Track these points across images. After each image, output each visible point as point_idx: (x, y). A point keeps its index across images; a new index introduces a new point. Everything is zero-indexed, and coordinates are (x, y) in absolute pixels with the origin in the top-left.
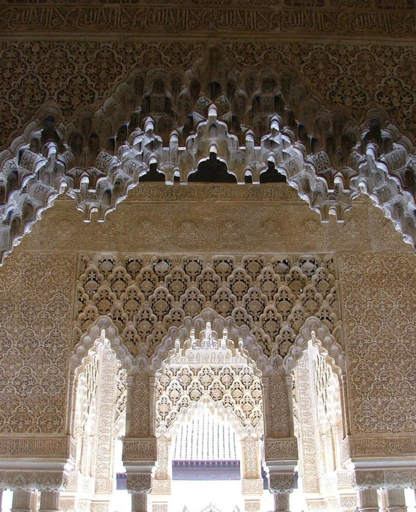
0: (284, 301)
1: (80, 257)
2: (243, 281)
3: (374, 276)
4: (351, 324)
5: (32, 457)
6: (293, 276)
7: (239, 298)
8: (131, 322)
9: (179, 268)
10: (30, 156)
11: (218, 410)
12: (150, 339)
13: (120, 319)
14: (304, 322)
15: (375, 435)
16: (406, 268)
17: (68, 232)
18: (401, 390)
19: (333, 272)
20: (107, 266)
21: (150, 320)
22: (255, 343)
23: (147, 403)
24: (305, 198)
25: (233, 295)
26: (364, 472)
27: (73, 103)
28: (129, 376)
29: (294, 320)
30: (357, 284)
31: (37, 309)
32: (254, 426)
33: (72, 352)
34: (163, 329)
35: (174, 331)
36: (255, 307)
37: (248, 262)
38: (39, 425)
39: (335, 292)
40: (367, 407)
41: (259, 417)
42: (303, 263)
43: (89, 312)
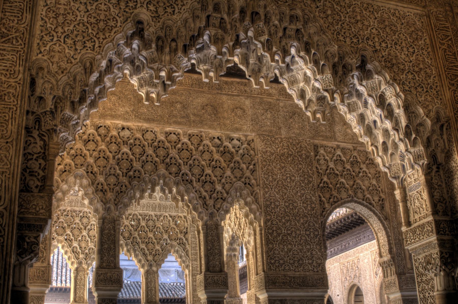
0: (218, 168)
2: (187, 150)
3: (283, 155)
4: (267, 190)
6: (224, 150)
7: (185, 163)
8: (101, 176)
10: (122, 49)
11: (127, 247)
13: (92, 172)
15: (283, 273)
16: (305, 151)
18: (300, 241)
22: (196, 199)
24: (301, 103)
25: (180, 161)
26: (274, 300)
27: (159, 13)
29: (225, 183)
30: (271, 160)
34: (127, 183)
36: (197, 171)
39: (254, 165)
40: (277, 252)
41: (159, 254)
43: (66, 165)
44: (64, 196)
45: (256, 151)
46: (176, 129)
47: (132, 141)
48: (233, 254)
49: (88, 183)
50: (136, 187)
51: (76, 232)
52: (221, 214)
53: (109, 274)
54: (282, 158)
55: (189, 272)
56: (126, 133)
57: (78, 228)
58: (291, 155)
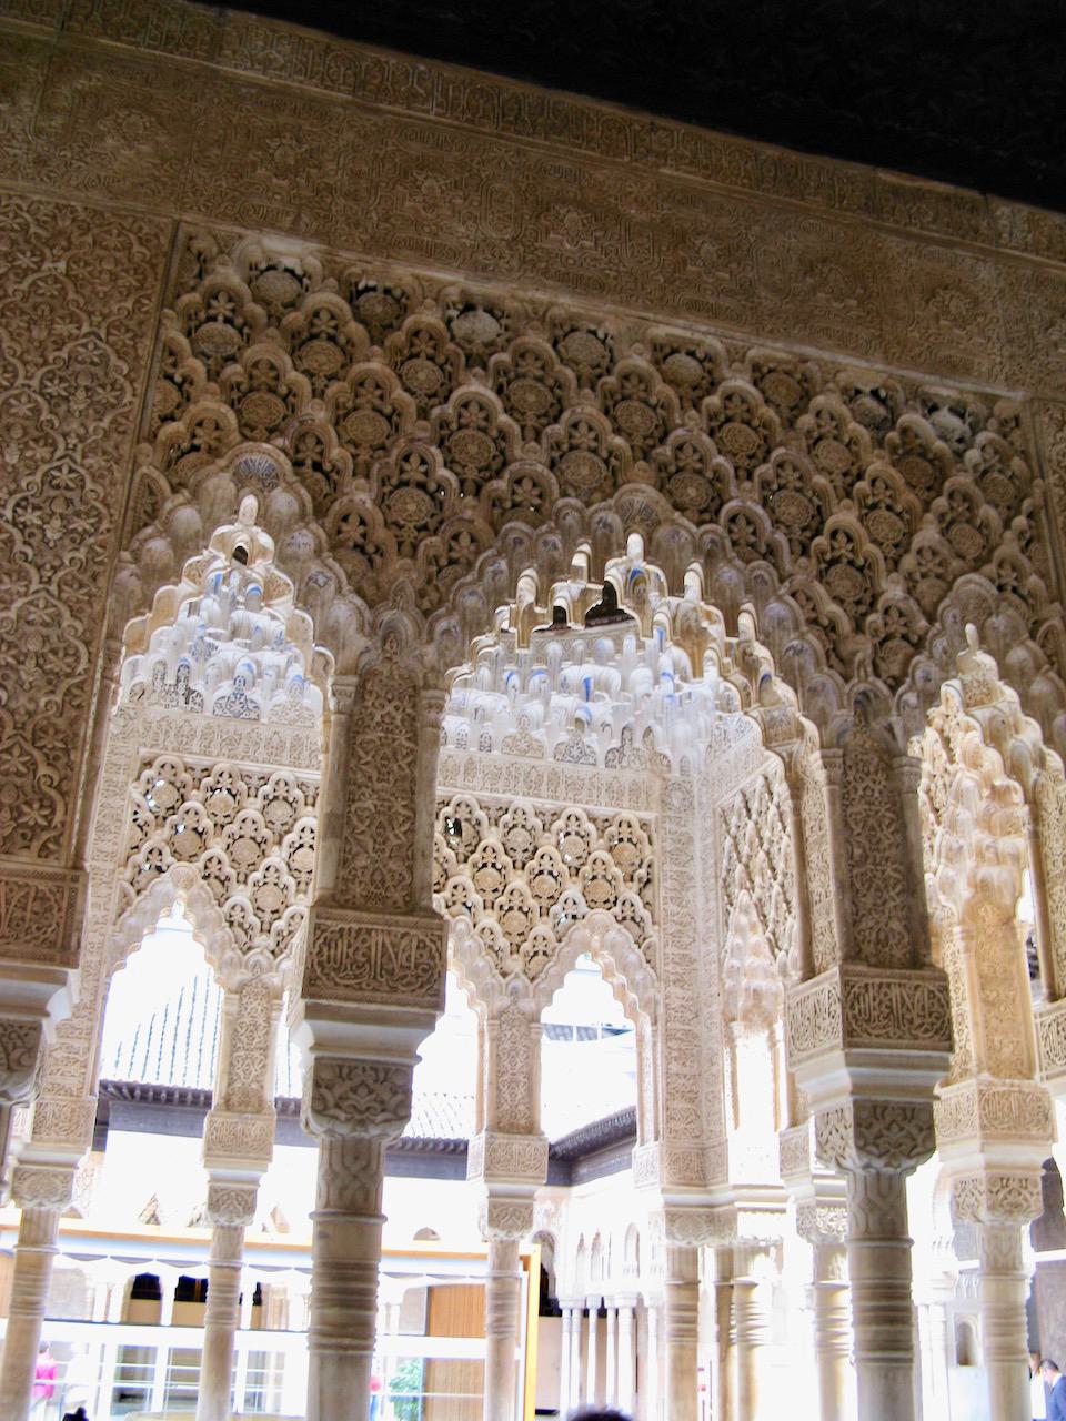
1: (181, 236)
2: (748, 423)
13: (317, 466)
14: (950, 588)
17: (145, 148)
19: (1025, 455)
20: (281, 287)
22: (797, 628)
23: (407, 785)
25: (720, 459)
28: (342, 672)
29: (918, 576)
32: (533, 979)
33: (126, 555)
34: (481, 524)
35: (518, 542)
36: (793, 510)
41: (545, 953)
43: (200, 424)
45: (1034, 463)
46: (697, 336)
47: (505, 357)
49: (296, 507)
50: (521, 549)
51: (246, 850)
52: (906, 702)
53: (377, 939)
55: (655, 1023)
56: (479, 326)
57: (253, 839)
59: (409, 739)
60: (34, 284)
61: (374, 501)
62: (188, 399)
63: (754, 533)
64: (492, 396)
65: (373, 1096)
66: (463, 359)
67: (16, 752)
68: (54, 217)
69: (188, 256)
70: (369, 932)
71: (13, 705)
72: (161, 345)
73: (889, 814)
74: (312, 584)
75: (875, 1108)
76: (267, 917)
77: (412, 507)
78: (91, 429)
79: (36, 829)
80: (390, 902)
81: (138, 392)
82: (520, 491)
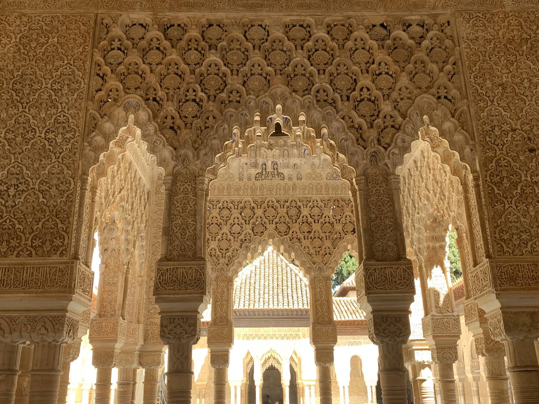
0: (384, 75)
1: (99, 19)
2: (325, 50)
3: (511, 41)
5: (20, 292)
7: (321, 72)
9: (237, 33)
12: (198, 126)
13: (154, 99)
14: (413, 103)
20: (137, 32)
21: (198, 100)
22: (344, 131)
23: (193, 213)
25: (312, 68)
26: (515, 313)
29: (399, 100)
31: (36, 86)
35: (231, 116)
36: (343, 83)
37: (332, 26)
38: (32, 246)
39: (454, 64)
40: (512, 218)
41: (330, 254)
42: (408, 27)
44: (108, 142)
45: (456, 40)
46: (303, 18)
47: (224, 43)
48: (438, 245)
50: (233, 118)
52: (393, 154)
53: (180, 271)
54: (509, 46)
58: (527, 40)
59: (194, 196)
60: (46, 48)
61: (175, 110)
62: (106, 82)
63: (327, 96)
64: (219, 60)
65: (182, 328)
66: (208, 47)
67: (50, 220)
68: (52, 21)
69: (102, 26)
70: (177, 268)
71: (49, 204)
72: (94, 63)
73: (387, 199)
74: (155, 144)
75: (383, 318)
76: (224, 252)
77: (190, 109)
78: (70, 99)
79: (58, 247)
80: (187, 256)
81: (86, 82)
82: (231, 96)
